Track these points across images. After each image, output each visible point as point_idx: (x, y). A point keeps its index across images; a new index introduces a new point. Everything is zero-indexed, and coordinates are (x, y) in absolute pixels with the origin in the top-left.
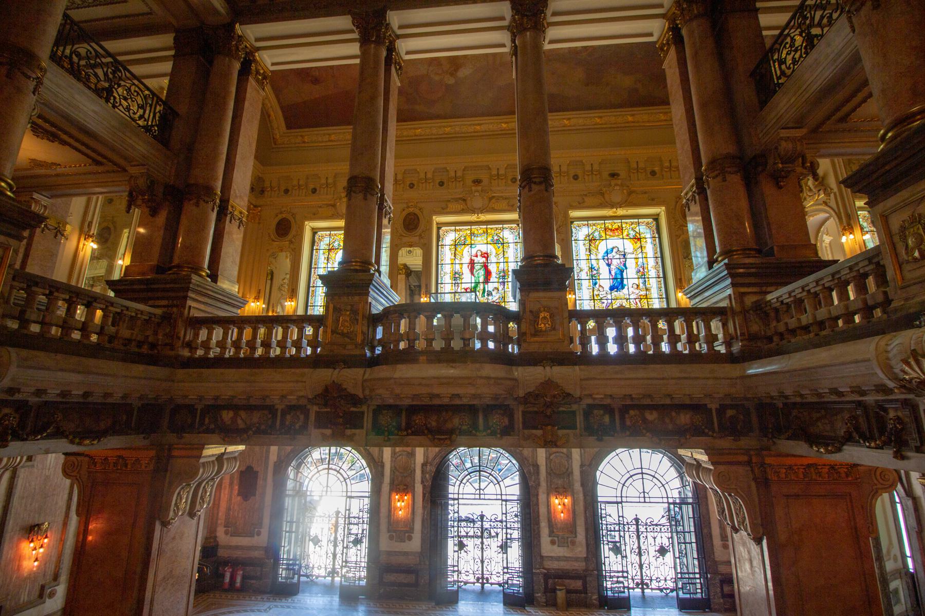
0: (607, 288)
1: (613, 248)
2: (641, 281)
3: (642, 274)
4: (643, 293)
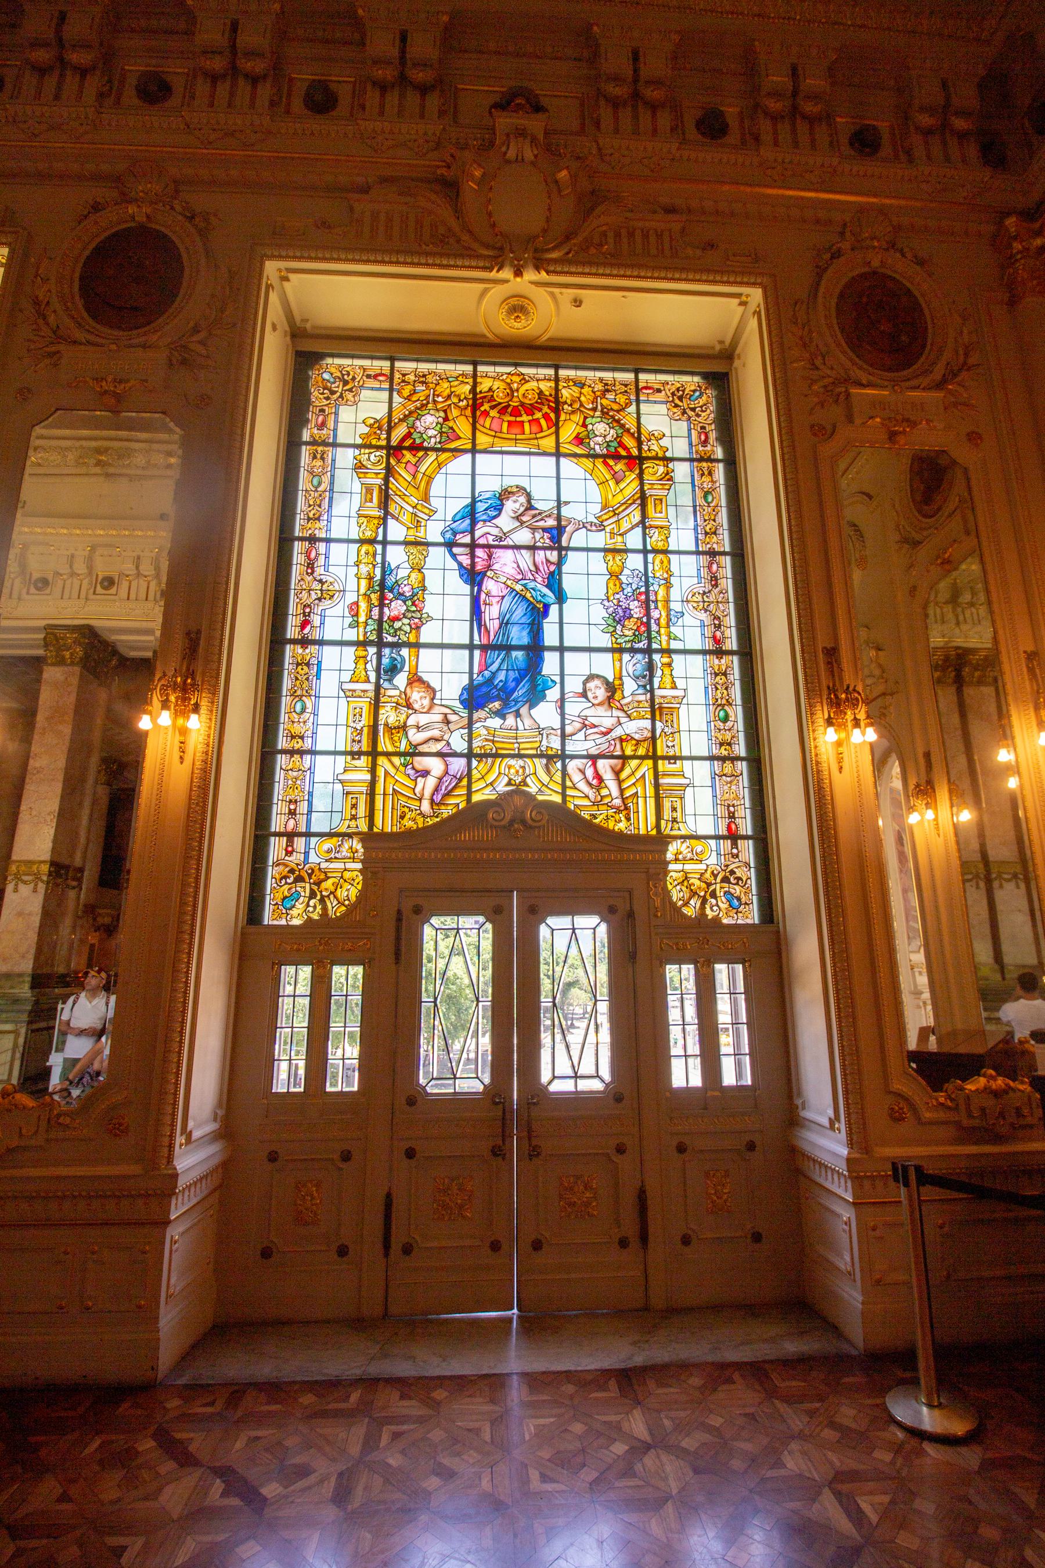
0: (451, 688)
1: (504, 495)
2: (632, 664)
3: (638, 629)
4: (637, 727)
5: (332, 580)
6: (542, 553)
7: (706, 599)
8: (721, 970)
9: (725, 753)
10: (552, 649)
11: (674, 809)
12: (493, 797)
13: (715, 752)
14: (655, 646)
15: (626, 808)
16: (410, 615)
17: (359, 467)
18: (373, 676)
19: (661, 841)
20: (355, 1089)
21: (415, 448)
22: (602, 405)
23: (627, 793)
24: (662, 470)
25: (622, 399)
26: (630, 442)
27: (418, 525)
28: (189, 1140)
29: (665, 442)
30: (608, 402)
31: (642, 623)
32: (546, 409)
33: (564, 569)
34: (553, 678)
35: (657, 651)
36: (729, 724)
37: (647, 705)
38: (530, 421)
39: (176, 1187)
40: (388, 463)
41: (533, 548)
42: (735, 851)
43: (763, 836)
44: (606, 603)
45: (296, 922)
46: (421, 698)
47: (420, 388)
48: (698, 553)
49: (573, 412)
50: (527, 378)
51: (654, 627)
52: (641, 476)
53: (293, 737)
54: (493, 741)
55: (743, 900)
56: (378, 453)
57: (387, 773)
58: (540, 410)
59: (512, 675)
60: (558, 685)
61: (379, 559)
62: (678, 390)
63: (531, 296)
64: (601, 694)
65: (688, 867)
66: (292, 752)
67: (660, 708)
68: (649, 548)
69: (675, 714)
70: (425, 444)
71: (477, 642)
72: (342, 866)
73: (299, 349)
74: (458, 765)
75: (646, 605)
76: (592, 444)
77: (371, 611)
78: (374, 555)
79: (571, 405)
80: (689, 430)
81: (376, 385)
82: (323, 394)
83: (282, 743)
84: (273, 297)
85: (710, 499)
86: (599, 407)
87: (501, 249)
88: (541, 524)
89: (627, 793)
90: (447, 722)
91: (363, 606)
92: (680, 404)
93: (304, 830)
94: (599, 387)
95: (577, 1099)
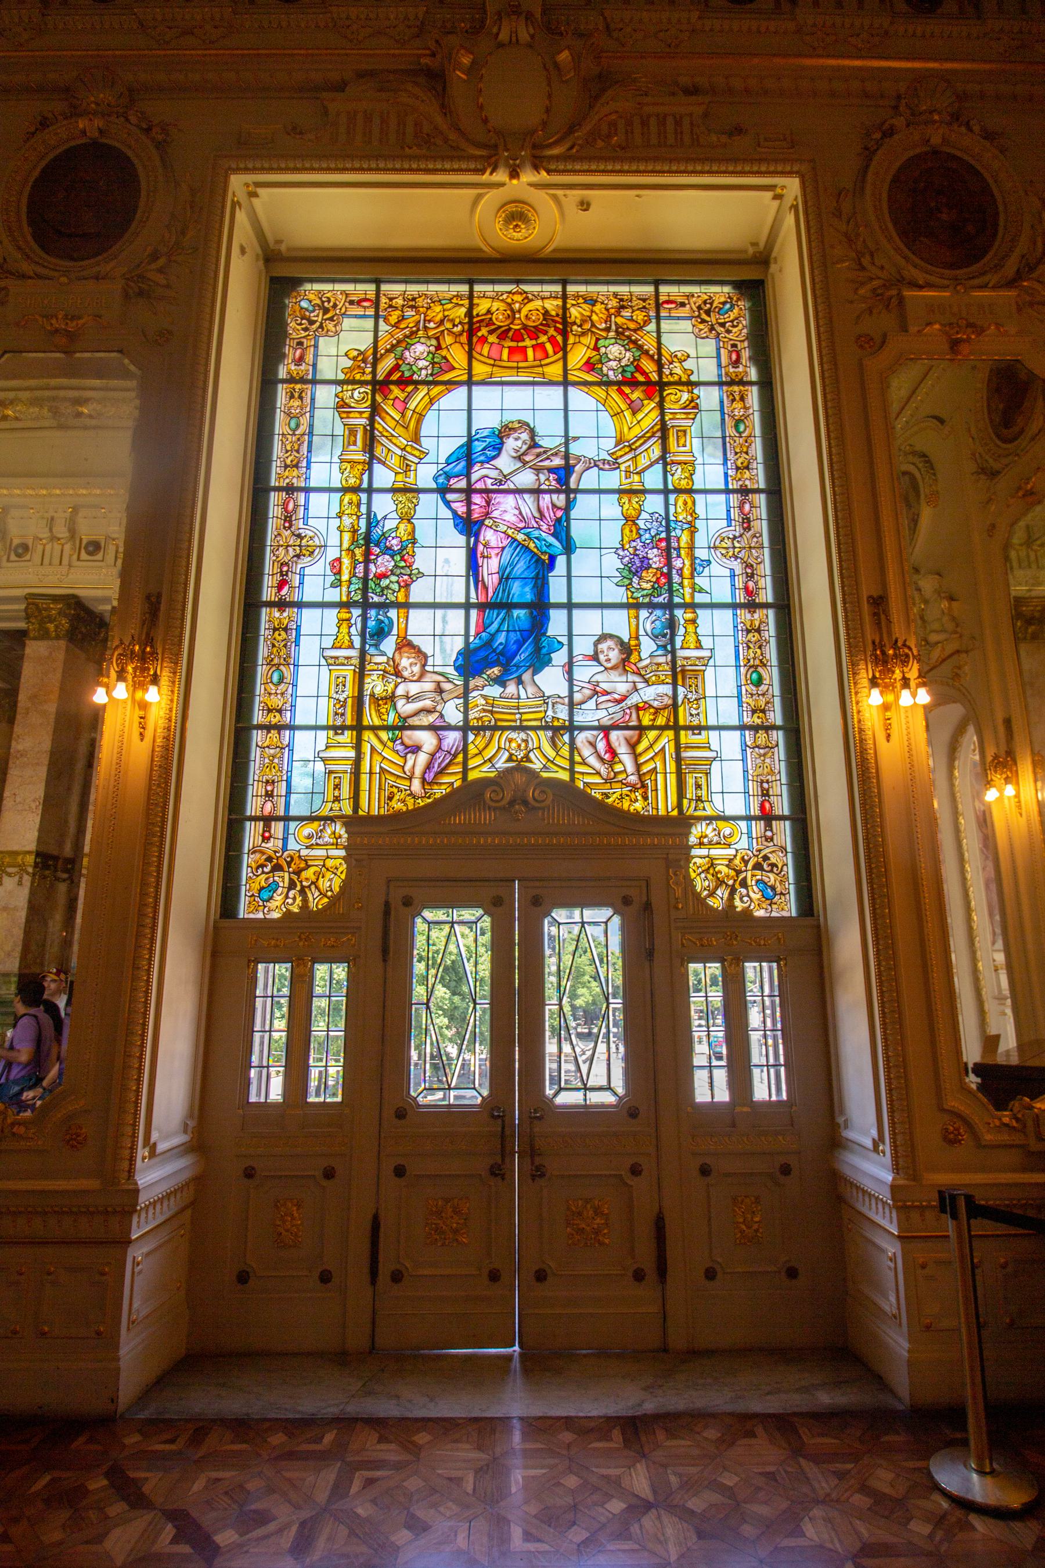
3: (658, 580)
5: (311, 534)
6: (547, 497)
7: (737, 545)
8: (751, 969)
9: (759, 721)
10: (558, 606)
11: (698, 786)
12: (492, 775)
13: (747, 720)
14: (677, 600)
15: (644, 786)
16: (398, 572)
17: (342, 407)
18: (357, 641)
19: (682, 823)
20: (339, 1099)
21: (403, 383)
22: (616, 324)
23: (645, 769)
24: (685, 396)
25: (640, 316)
26: (649, 366)
27: (407, 469)
28: (153, 1154)
29: (689, 364)
30: (624, 321)
31: (662, 574)
32: (552, 332)
33: (573, 514)
34: (560, 639)
35: (679, 606)
36: (763, 688)
37: (667, 668)
38: (533, 346)
39: (137, 1204)
40: (374, 400)
41: (537, 492)
42: (769, 834)
43: (801, 816)
44: (621, 552)
45: (276, 915)
46: (411, 665)
47: (409, 313)
48: (727, 491)
49: (583, 334)
50: (530, 296)
51: (676, 578)
52: (661, 405)
53: (270, 711)
54: (492, 712)
55: (778, 890)
56: (362, 390)
57: (373, 749)
58: (545, 333)
59: (513, 637)
60: (566, 647)
61: (364, 509)
62: (705, 302)
63: (529, 201)
64: (615, 656)
65: (713, 852)
66: (268, 728)
67: (683, 671)
68: (670, 487)
69: (700, 678)
70: (415, 377)
71: (473, 600)
72: (323, 853)
73: (275, 275)
74: (452, 738)
75: (667, 555)
76: (605, 369)
77: (355, 568)
78: (359, 505)
79: (580, 326)
80: (718, 349)
81: (360, 311)
82: (301, 324)
83: (258, 717)
84: (241, 216)
85: (742, 428)
86: (613, 327)
87: (496, 146)
88: (547, 463)
89: (645, 769)
90: (440, 691)
91: (346, 562)
92: (708, 319)
93: (282, 814)
94: (614, 303)
95: (585, 1113)
